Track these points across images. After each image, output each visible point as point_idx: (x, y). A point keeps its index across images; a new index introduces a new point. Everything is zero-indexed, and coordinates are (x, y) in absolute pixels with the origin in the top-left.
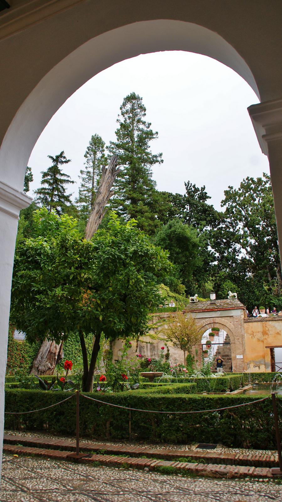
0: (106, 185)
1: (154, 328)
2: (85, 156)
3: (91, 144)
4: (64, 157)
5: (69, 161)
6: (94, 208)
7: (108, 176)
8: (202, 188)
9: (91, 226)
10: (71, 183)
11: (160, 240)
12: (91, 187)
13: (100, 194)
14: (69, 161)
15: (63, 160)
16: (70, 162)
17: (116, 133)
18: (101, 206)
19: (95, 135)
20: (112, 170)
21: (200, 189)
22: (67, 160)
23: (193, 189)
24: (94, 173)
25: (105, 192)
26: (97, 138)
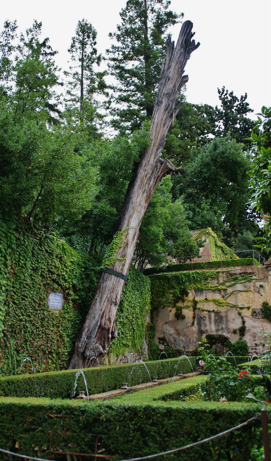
0: (177, 67)
1: (220, 291)
2: (69, 51)
3: (77, 33)
4: (49, 47)
5: (55, 52)
6: (161, 103)
7: (179, 52)
8: (242, 96)
9: (158, 129)
10: (60, 86)
11: (201, 166)
12: (79, 95)
13: (169, 80)
14: (55, 52)
15: (48, 51)
16: (57, 54)
17: (121, 15)
18: (171, 99)
19: (83, 21)
20: (185, 43)
21: (239, 98)
22: (54, 50)
23: (229, 98)
24: (82, 75)
25: (176, 77)
26: (86, 24)
